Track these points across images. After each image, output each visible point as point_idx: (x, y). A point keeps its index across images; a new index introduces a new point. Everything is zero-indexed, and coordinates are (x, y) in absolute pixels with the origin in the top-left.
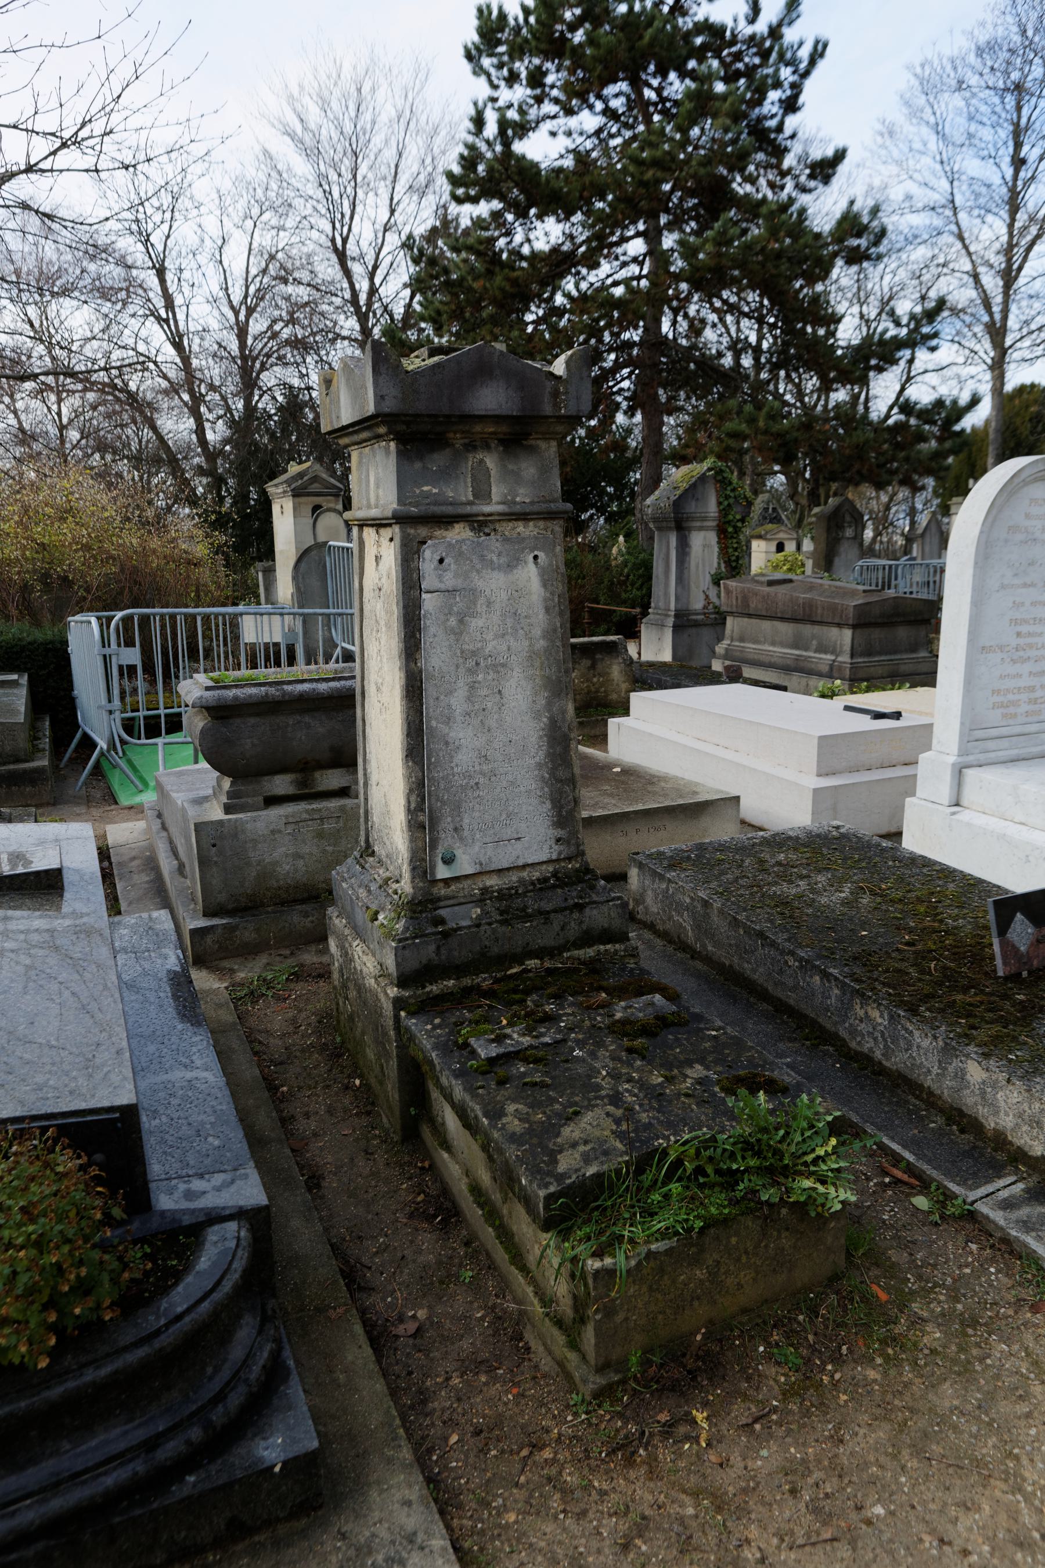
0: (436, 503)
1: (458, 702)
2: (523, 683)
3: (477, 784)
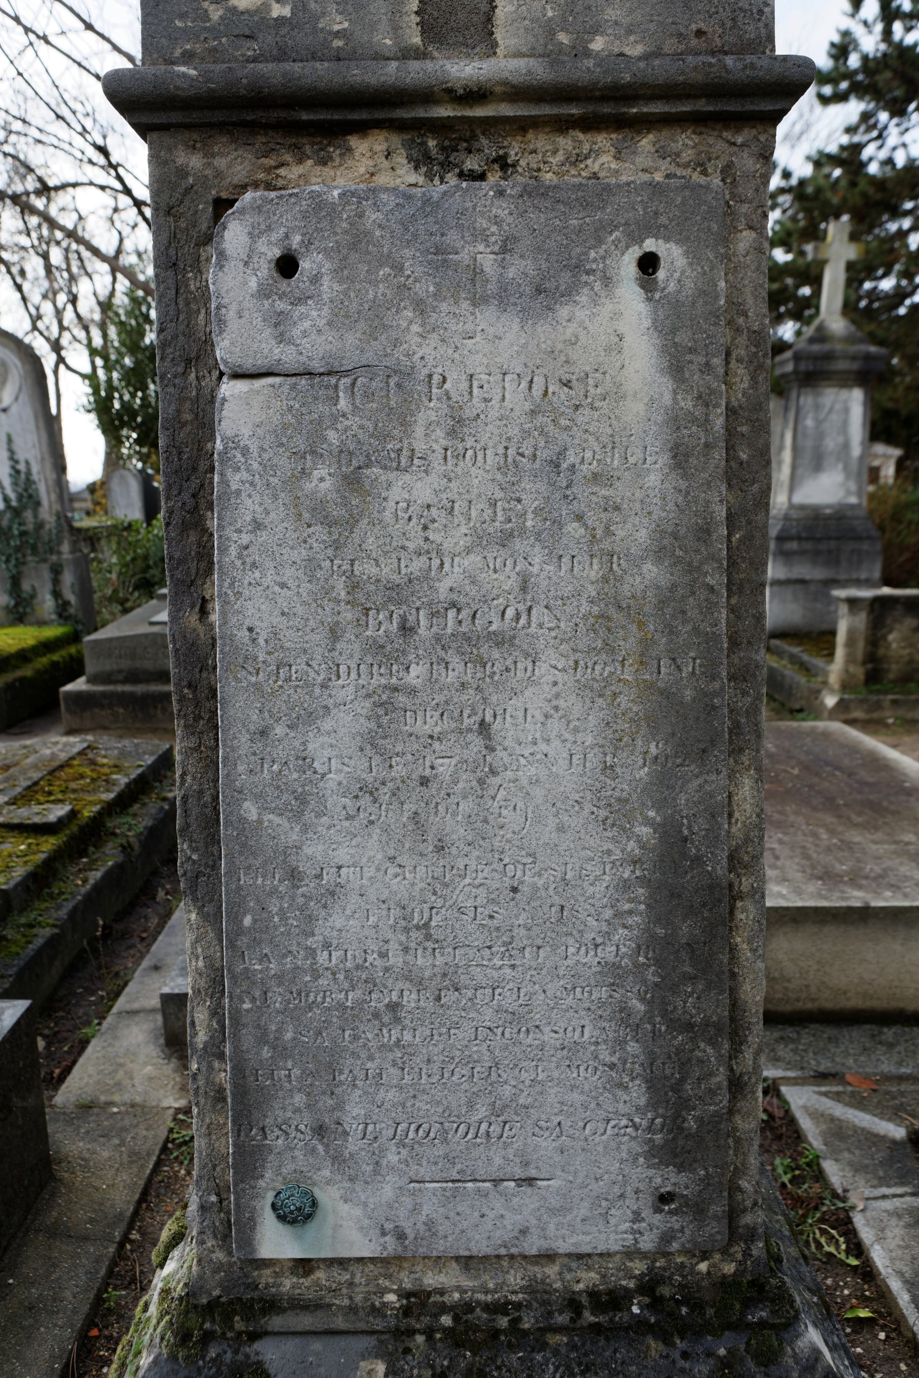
0: (282, 55)
1: (335, 746)
2: (573, 704)
3: (393, 1007)
